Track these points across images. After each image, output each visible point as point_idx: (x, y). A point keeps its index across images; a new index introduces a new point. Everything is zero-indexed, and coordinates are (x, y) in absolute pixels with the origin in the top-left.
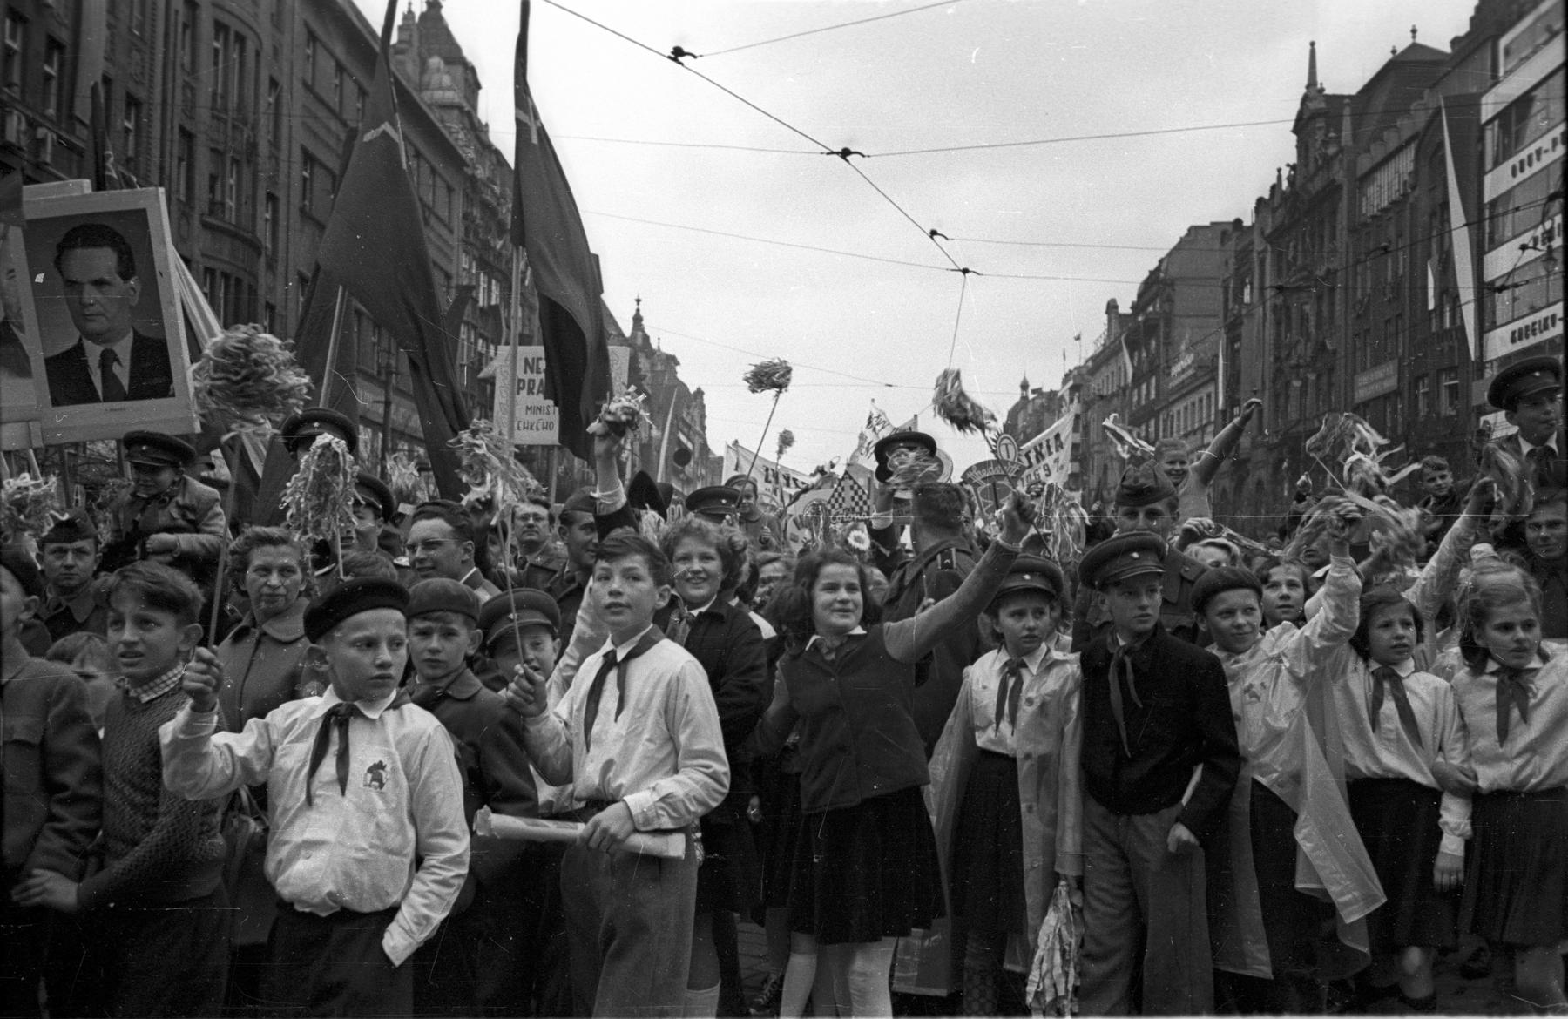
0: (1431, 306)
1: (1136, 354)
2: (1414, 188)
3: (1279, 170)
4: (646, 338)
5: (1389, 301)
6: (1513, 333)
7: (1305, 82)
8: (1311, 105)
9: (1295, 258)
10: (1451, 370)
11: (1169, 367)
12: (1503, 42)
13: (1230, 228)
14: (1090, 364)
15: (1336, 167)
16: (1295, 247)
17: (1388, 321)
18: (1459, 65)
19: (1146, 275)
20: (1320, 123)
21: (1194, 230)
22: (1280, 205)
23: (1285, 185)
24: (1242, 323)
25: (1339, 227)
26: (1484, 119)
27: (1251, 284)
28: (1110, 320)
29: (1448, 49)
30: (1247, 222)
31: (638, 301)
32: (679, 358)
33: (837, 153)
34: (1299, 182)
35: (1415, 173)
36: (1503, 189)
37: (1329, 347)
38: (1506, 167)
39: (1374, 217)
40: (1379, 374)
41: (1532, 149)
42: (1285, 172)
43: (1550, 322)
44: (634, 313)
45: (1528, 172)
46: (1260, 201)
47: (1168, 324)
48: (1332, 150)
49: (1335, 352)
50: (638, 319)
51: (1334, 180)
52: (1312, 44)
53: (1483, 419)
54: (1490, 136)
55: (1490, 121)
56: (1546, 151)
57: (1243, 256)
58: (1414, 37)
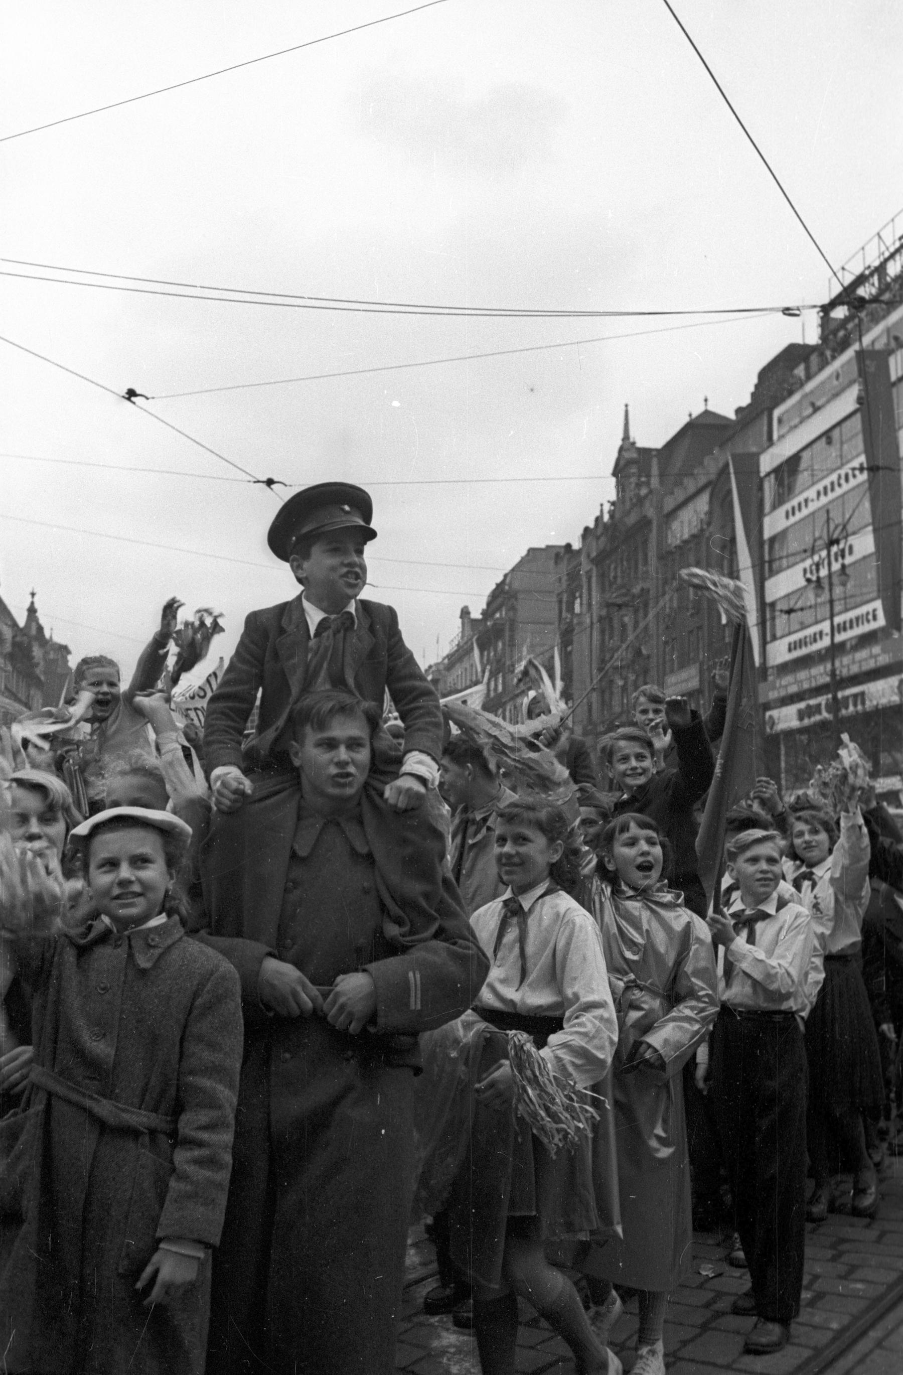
1: (486, 653)
2: (709, 524)
3: (602, 505)
4: (40, 629)
5: (692, 615)
6: (790, 644)
7: (620, 435)
8: (627, 455)
9: (615, 577)
11: (513, 666)
12: (777, 413)
13: (562, 551)
14: (446, 661)
15: (647, 504)
16: (616, 568)
17: (691, 632)
18: (742, 429)
19: (494, 586)
20: (634, 470)
21: (532, 551)
22: (602, 534)
23: (606, 518)
24: (573, 630)
25: (650, 554)
26: (762, 474)
27: (581, 597)
28: (463, 624)
29: (732, 416)
30: (576, 545)
31: (33, 594)
32: (71, 647)
33: (263, 482)
34: (617, 516)
35: (710, 513)
37: (644, 652)
38: (782, 511)
39: (679, 547)
40: (684, 675)
41: (801, 498)
42: (607, 507)
43: (818, 636)
44: (27, 605)
45: (798, 516)
46: (587, 529)
47: (512, 630)
48: (644, 491)
49: (648, 657)
50: (32, 611)
51: (645, 517)
52: (626, 406)
53: (768, 714)
54: (769, 487)
55: (768, 474)
56: (812, 500)
57: (573, 576)
58: (706, 405)
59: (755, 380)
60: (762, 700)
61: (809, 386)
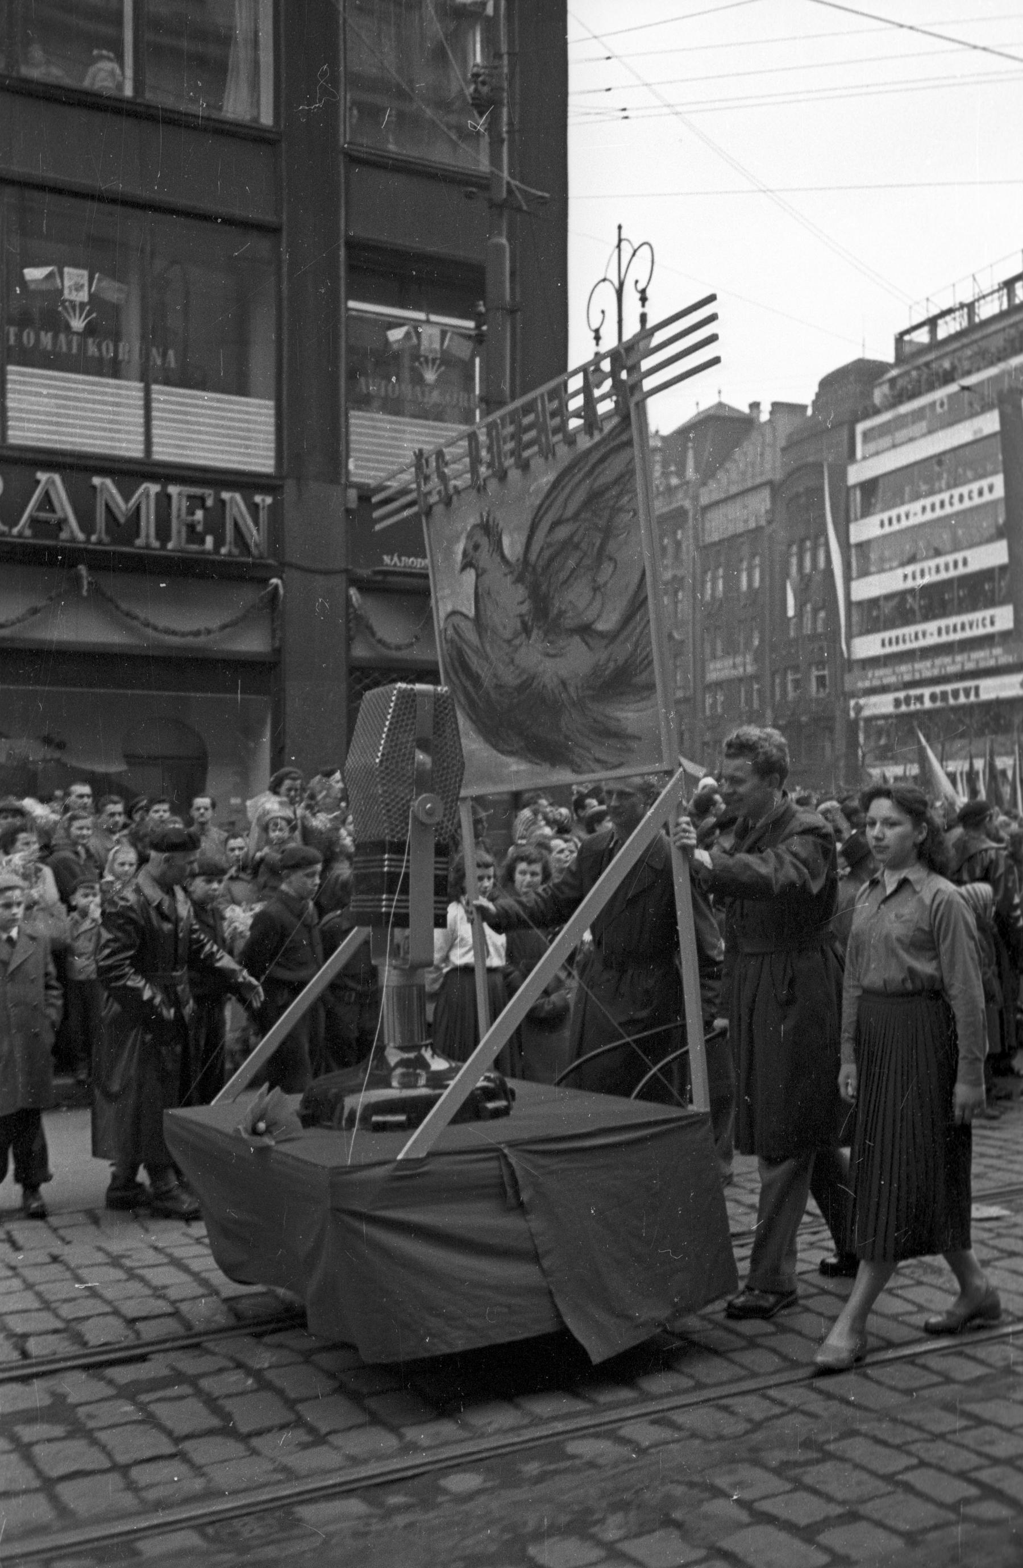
0: (791, 613)
10: (821, 664)
12: (860, 428)
35: (772, 512)
36: (864, 537)
49: (682, 642)
51: (682, 507)
59: (815, 389)
60: (848, 687)
61: (904, 409)
